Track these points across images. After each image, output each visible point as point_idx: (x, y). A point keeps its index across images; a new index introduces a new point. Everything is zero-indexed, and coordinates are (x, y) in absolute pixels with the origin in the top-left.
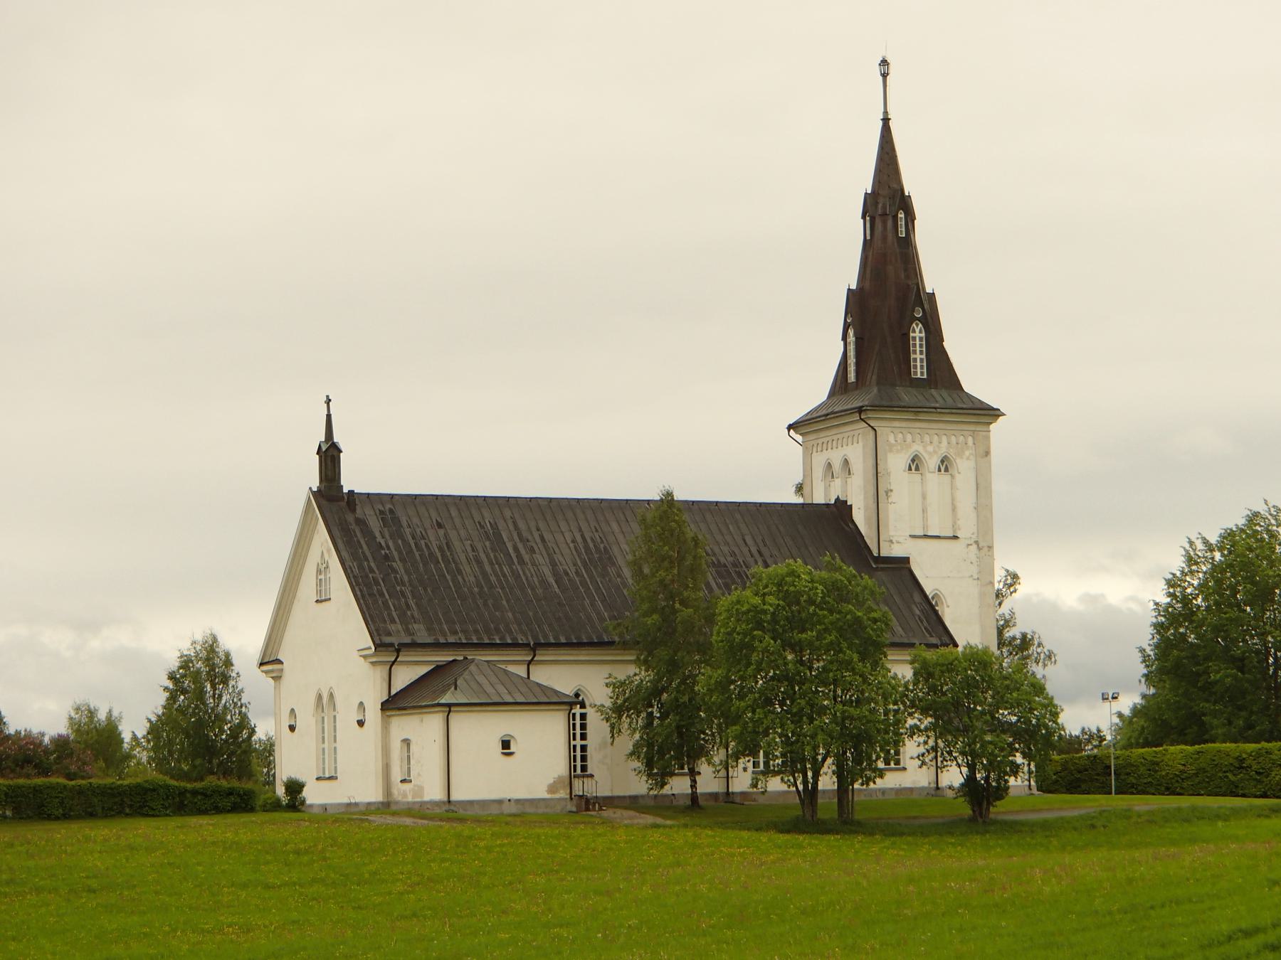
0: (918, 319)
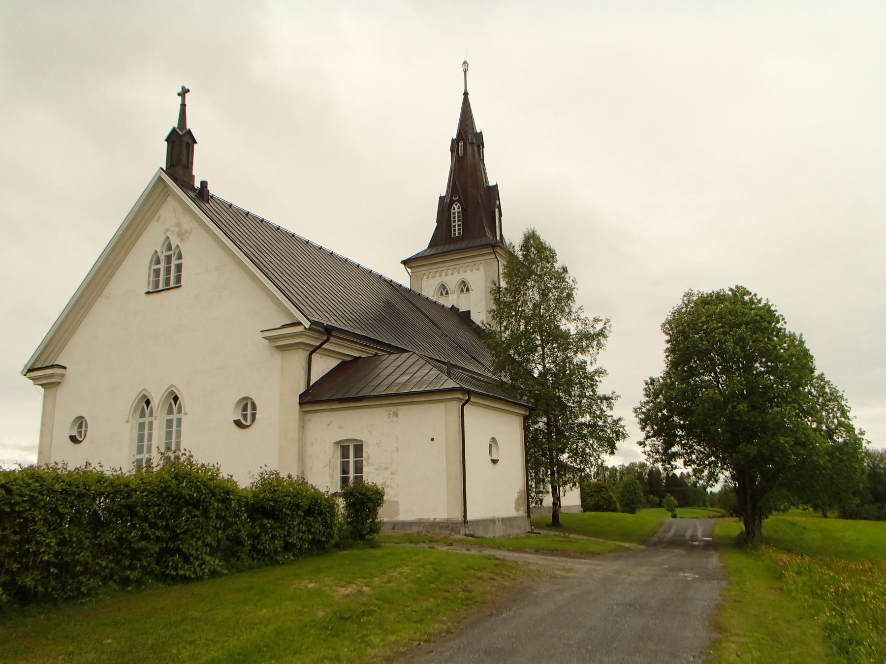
0: (455, 201)
